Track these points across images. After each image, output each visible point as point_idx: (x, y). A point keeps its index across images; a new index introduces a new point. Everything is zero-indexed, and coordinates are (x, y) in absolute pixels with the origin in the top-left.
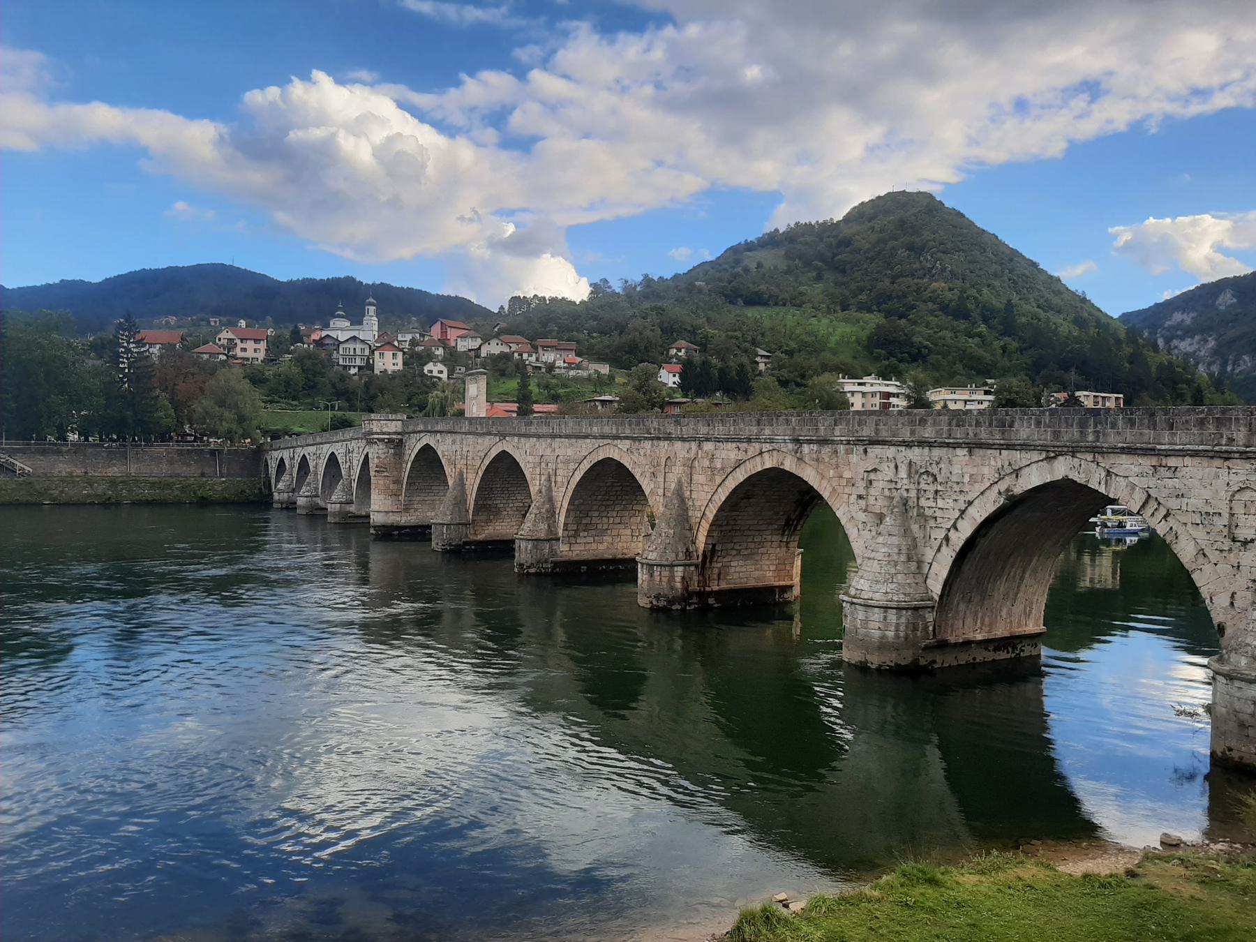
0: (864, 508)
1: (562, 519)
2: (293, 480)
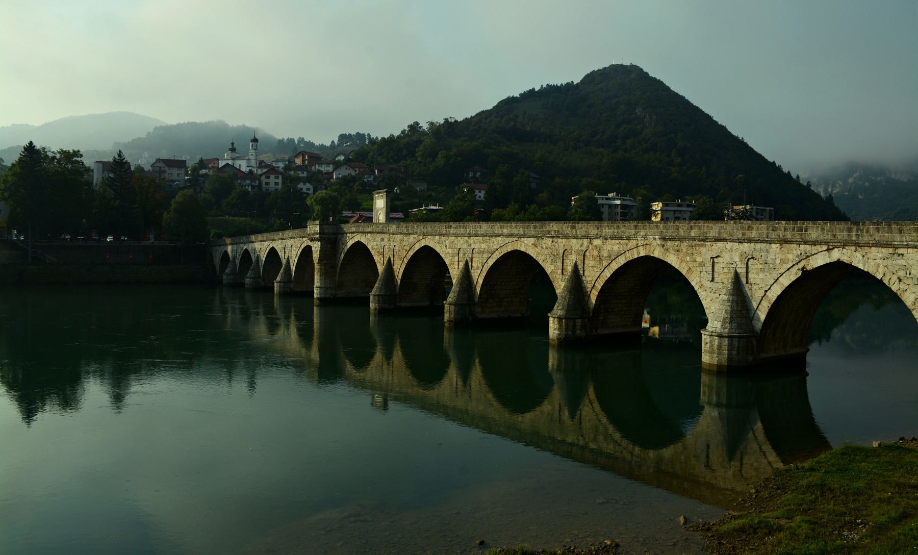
0: (711, 279)
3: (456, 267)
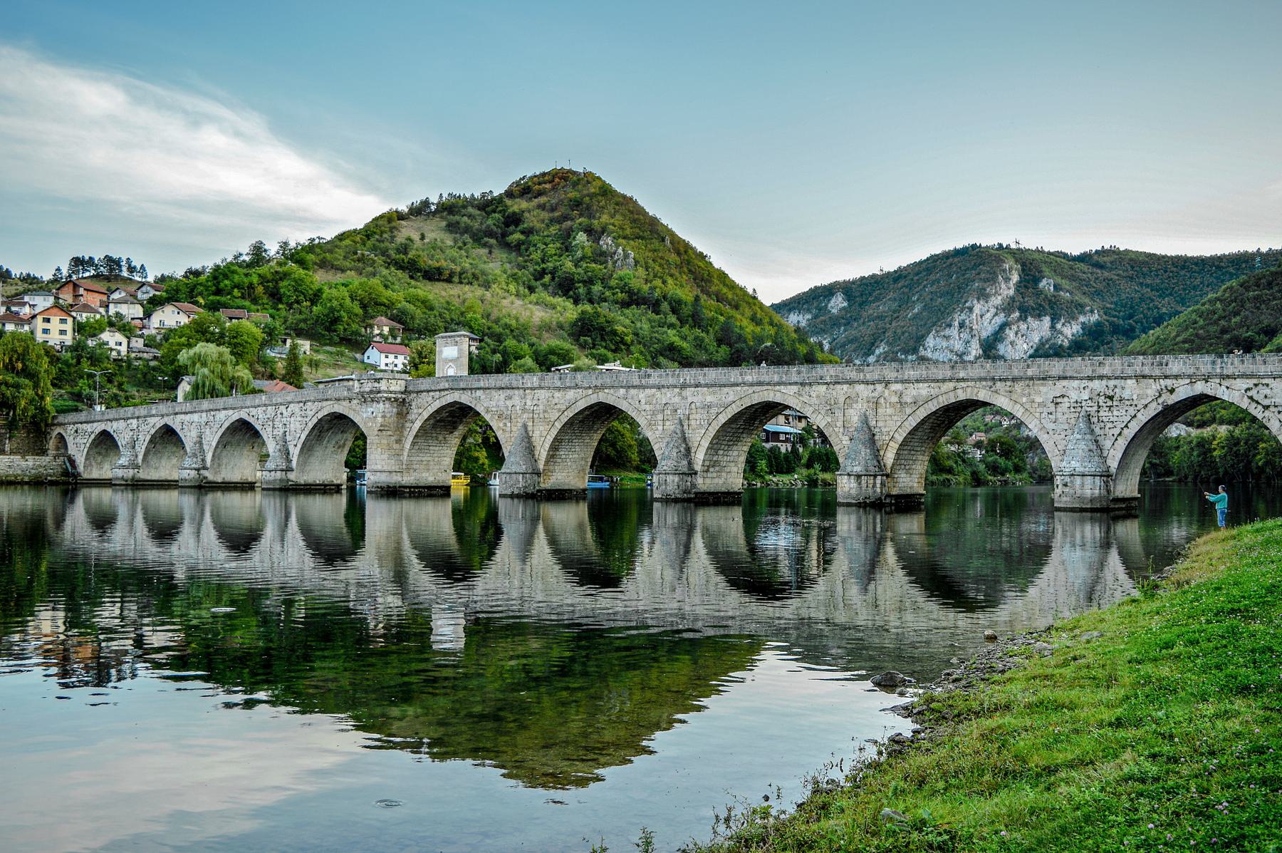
1: (699, 457)
2: (137, 456)
3: (660, 428)
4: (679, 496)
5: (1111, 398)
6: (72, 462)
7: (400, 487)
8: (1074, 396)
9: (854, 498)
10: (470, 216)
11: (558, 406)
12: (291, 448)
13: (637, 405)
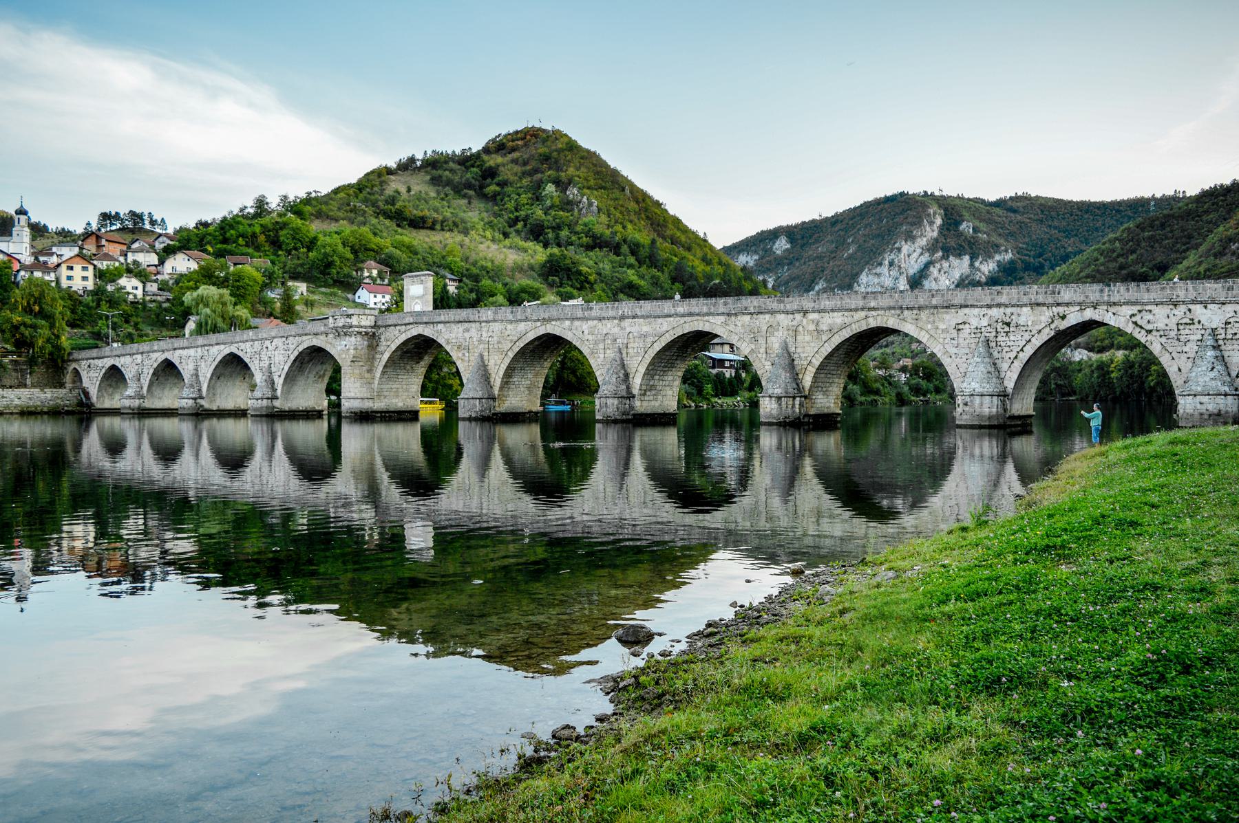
1: (637, 382)
3: (602, 356)
4: (618, 417)
5: (1008, 324)
6: (86, 394)
7: (372, 412)
8: (974, 322)
9: (775, 418)
10: (451, 170)
11: (511, 337)
12: (276, 379)
13: (581, 335)
